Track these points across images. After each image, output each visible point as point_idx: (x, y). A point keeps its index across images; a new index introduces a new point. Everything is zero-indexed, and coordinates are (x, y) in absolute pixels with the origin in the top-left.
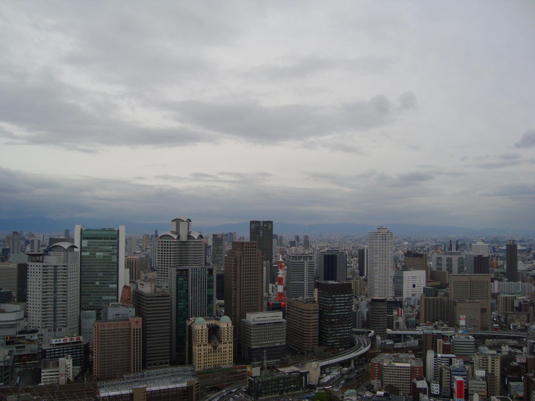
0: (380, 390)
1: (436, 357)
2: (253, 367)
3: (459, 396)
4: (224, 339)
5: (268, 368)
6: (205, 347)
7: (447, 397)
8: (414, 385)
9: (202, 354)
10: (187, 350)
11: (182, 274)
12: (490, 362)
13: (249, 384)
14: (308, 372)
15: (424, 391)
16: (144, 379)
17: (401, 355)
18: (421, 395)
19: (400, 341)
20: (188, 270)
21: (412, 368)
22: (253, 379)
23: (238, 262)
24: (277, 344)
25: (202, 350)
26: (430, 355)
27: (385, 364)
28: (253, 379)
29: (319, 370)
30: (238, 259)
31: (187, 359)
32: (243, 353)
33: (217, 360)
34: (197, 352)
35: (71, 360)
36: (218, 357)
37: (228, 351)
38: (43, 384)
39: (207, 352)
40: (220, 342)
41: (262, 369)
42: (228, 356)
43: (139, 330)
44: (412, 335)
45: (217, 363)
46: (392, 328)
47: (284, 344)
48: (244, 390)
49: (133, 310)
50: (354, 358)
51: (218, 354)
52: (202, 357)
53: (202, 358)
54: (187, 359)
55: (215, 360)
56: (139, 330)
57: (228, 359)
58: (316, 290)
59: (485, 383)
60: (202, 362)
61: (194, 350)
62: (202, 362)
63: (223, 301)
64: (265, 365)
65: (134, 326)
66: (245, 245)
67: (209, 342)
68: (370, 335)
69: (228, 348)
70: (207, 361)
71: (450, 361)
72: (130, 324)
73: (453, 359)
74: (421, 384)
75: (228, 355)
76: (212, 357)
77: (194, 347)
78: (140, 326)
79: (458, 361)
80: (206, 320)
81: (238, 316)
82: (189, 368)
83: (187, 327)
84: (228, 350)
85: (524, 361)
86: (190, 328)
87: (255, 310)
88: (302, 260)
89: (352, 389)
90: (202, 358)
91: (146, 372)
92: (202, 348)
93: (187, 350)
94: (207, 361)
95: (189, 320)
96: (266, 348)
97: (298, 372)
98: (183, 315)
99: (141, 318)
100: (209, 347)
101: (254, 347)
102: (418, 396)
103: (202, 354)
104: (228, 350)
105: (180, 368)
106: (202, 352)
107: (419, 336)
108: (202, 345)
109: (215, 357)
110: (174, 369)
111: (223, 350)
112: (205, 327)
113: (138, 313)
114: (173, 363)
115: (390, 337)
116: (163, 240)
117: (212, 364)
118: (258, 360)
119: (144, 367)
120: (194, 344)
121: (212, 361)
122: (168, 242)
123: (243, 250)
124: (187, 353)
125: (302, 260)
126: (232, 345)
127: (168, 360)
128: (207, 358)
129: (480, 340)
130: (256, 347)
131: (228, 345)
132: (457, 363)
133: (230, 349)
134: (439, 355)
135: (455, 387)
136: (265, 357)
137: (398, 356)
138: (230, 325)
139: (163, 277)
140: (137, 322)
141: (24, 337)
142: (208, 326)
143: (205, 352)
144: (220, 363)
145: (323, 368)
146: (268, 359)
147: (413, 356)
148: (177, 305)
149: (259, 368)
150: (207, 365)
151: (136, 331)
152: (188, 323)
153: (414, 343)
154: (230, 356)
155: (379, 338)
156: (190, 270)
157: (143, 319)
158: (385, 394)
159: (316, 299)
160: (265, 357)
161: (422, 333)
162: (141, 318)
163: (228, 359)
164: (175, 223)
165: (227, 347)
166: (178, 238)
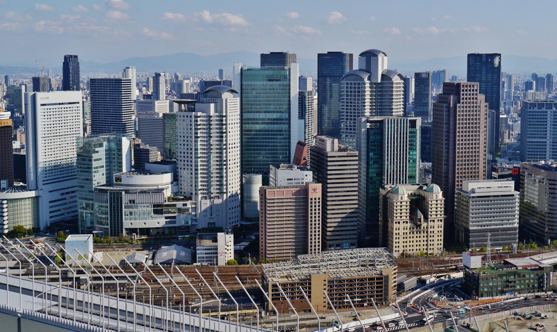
4: (432, 214)
5: (493, 258)
6: (405, 225)
9: (401, 234)
10: (381, 228)
16: (324, 264)
23: (452, 111)
24: (505, 226)
25: (401, 229)
28: (471, 272)
31: (381, 240)
32: (456, 237)
33: (422, 243)
34: (395, 232)
35: (232, 236)
36: (422, 239)
37: (436, 232)
38: (199, 264)
39: (408, 231)
40: (426, 219)
41: (483, 259)
42: (436, 238)
43: (317, 201)
48: (459, 286)
49: (310, 173)
51: (422, 234)
52: (401, 238)
53: (401, 240)
54: (381, 240)
55: (418, 243)
56: (317, 201)
60: (401, 244)
61: (390, 229)
62: (401, 244)
63: (429, 165)
65: (311, 195)
66: (462, 88)
67: (411, 219)
69: (436, 227)
70: (408, 244)
75: (436, 236)
76: (415, 239)
77: (390, 224)
78: (319, 195)
83: (381, 197)
86: (385, 198)
87: (475, 177)
88: (544, 109)
90: (401, 240)
92: (402, 225)
93: (381, 228)
94: (408, 244)
95: (384, 188)
96: (491, 230)
97: (538, 266)
99: (320, 185)
103: (401, 234)
104: (436, 229)
106: (401, 231)
108: (401, 222)
109: (418, 239)
111: (430, 230)
112: (406, 198)
114: (361, 244)
116: (349, 82)
118: (477, 246)
120: (390, 220)
121: (415, 243)
122: (355, 84)
123: (459, 95)
124: (381, 232)
125: (544, 109)
126: (442, 224)
127: (355, 241)
128: (408, 240)
131: (437, 223)
133: (440, 229)
136: (489, 243)
138: (440, 196)
139: (349, 131)
140: (315, 190)
141: (174, 205)
143: (405, 231)
146: (492, 245)
148: (368, 169)
149: (480, 257)
150: (408, 248)
151: (313, 201)
152: (382, 192)
154: (439, 238)
157: (323, 187)
160: (489, 243)
162: (320, 185)
163: (436, 242)
164: (364, 58)
165: (436, 226)
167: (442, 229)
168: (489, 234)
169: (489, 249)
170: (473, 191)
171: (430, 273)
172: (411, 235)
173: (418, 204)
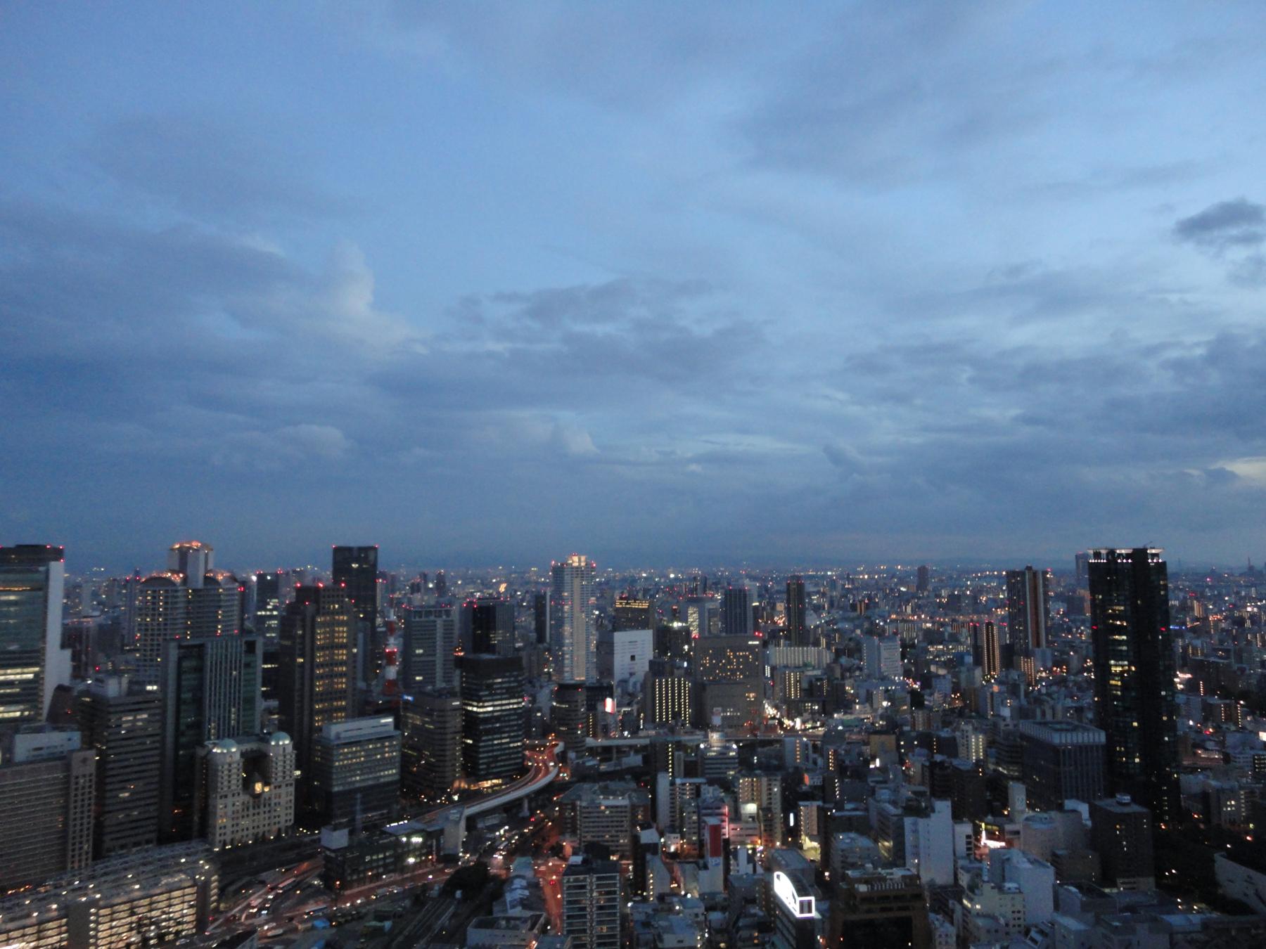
0: (575, 853)
1: (672, 784)
2: (335, 829)
3: (715, 853)
5: (365, 828)
7: (692, 857)
8: (635, 839)
11: (194, 653)
12: (764, 788)
13: (325, 866)
14: (441, 832)
15: (654, 848)
17: (613, 785)
18: (649, 857)
19: (610, 759)
20: (202, 646)
21: (634, 808)
22: (333, 855)
23: (308, 623)
24: (382, 780)
25: (230, 805)
26: (663, 781)
27: (584, 804)
28: (333, 855)
29: (463, 824)
30: (308, 620)
31: (196, 828)
36: (262, 816)
41: (351, 833)
44: (631, 747)
45: (261, 830)
46: (595, 736)
47: (397, 777)
49: (76, 736)
50: (527, 796)
51: (262, 809)
54: (196, 828)
57: (283, 819)
58: (458, 672)
59: (757, 825)
62: (229, 830)
63: (274, 703)
64: (359, 824)
65: (77, 769)
68: (557, 750)
69: (283, 796)
71: (697, 792)
72: (68, 768)
73: (703, 787)
74: (648, 836)
78: (91, 769)
79: (711, 789)
80: (239, 742)
81: (306, 732)
82: (197, 845)
84: (283, 800)
85: (818, 782)
88: (432, 618)
89: (523, 855)
91: (100, 868)
92: (230, 800)
98: (192, 736)
100: (244, 798)
101: (336, 789)
102: (644, 858)
105: (179, 848)
106: (230, 809)
107: (644, 748)
108: (230, 795)
110: (166, 851)
111: (273, 801)
112: (238, 757)
113: (88, 743)
114: (164, 839)
115: (593, 751)
117: (251, 831)
118: (342, 816)
119: (99, 853)
123: (317, 601)
125: (432, 618)
126: (292, 789)
127: (153, 836)
129: (748, 749)
130: (341, 788)
132: (710, 792)
134: (678, 781)
135: (707, 836)
136: (358, 808)
137: (606, 787)
140: (84, 761)
142: (243, 755)
144: (267, 828)
145: (471, 822)
147: (633, 785)
148: (178, 718)
149: (346, 831)
152: (201, 752)
153: (635, 760)
155: (572, 755)
156: (209, 645)
158: (584, 861)
159: (458, 689)
161: (647, 741)
166: (185, 581)
167: (292, 798)
168: (359, 796)
169: (358, 817)
170: (338, 737)
171: (272, 867)
172: (245, 813)
173: (256, 765)
